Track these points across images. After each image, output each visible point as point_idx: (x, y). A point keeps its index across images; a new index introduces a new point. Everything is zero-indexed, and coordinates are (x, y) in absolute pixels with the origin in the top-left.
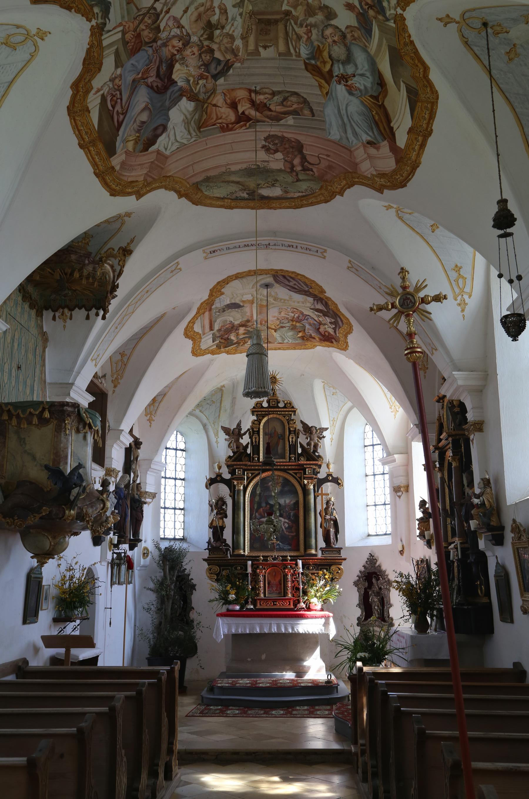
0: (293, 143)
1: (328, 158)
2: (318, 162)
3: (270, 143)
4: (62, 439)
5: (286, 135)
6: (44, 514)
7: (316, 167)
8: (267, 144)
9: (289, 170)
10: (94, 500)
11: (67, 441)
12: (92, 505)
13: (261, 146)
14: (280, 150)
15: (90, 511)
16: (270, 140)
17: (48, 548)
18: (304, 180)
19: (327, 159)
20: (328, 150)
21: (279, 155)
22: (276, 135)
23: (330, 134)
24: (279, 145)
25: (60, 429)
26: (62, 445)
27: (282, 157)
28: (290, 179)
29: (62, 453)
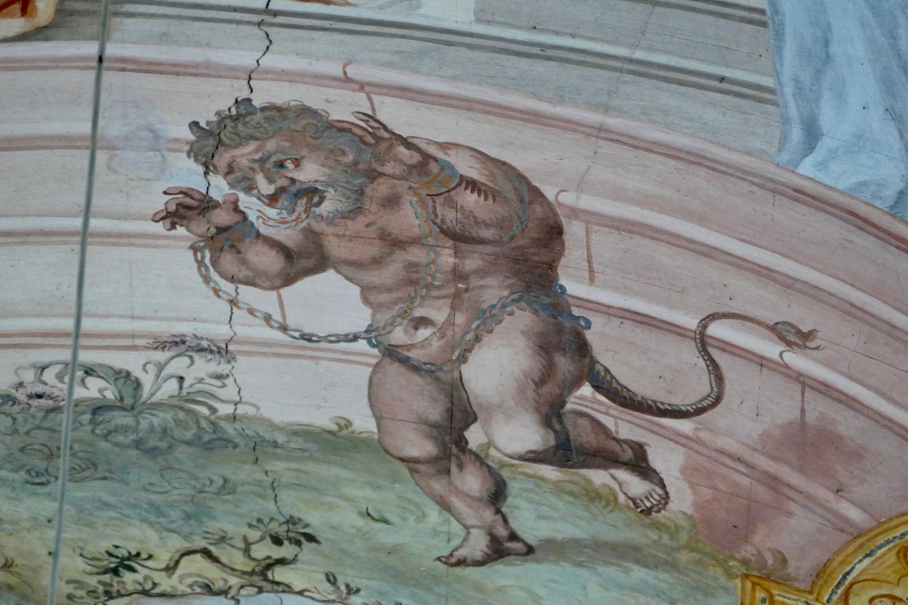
0: (470, 199)
1: (796, 360)
2: (698, 386)
3: (250, 188)
5: (398, 116)
7: (678, 438)
8: (219, 188)
9: (420, 447)
13: (160, 203)
14: (335, 248)
16: (245, 154)
18: (556, 549)
19: (785, 371)
20: (789, 284)
21: (331, 301)
22: (305, 111)
23: (812, 135)
24: (326, 208)
27: (359, 317)
28: (428, 527)
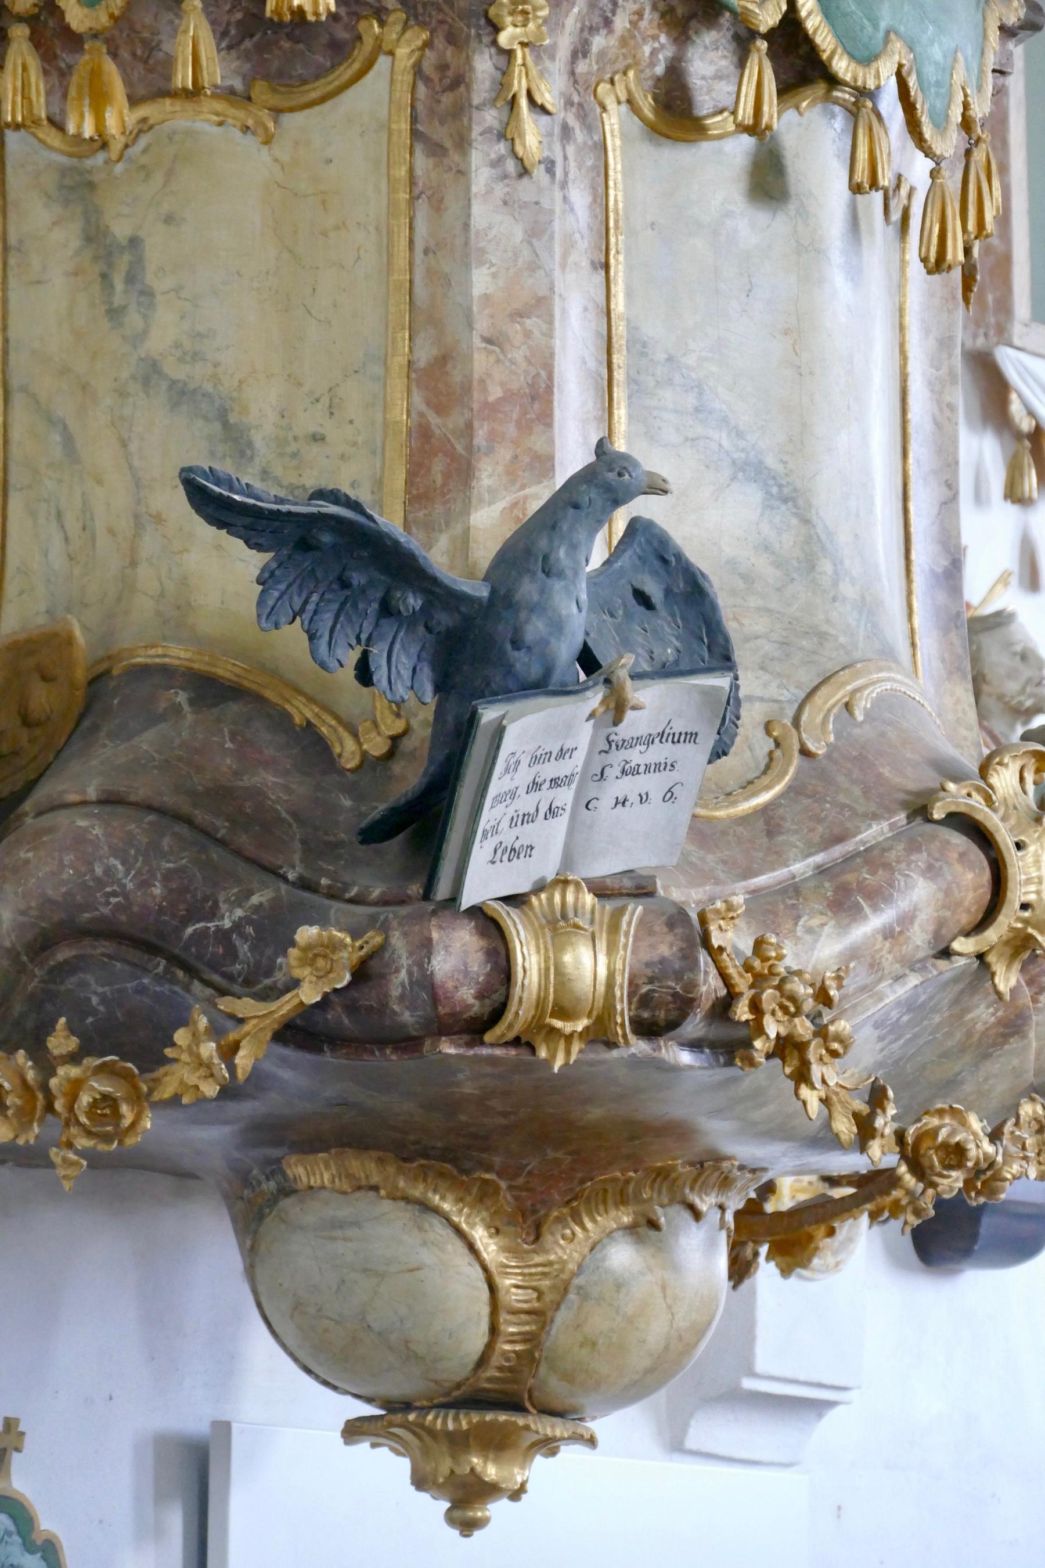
4: (481, 214)
6: (309, 994)
10: (874, 832)
11: (538, 230)
12: (845, 892)
15: (815, 949)
17: (476, 1340)
25: (441, 114)
26: (481, 281)
29: (481, 362)
